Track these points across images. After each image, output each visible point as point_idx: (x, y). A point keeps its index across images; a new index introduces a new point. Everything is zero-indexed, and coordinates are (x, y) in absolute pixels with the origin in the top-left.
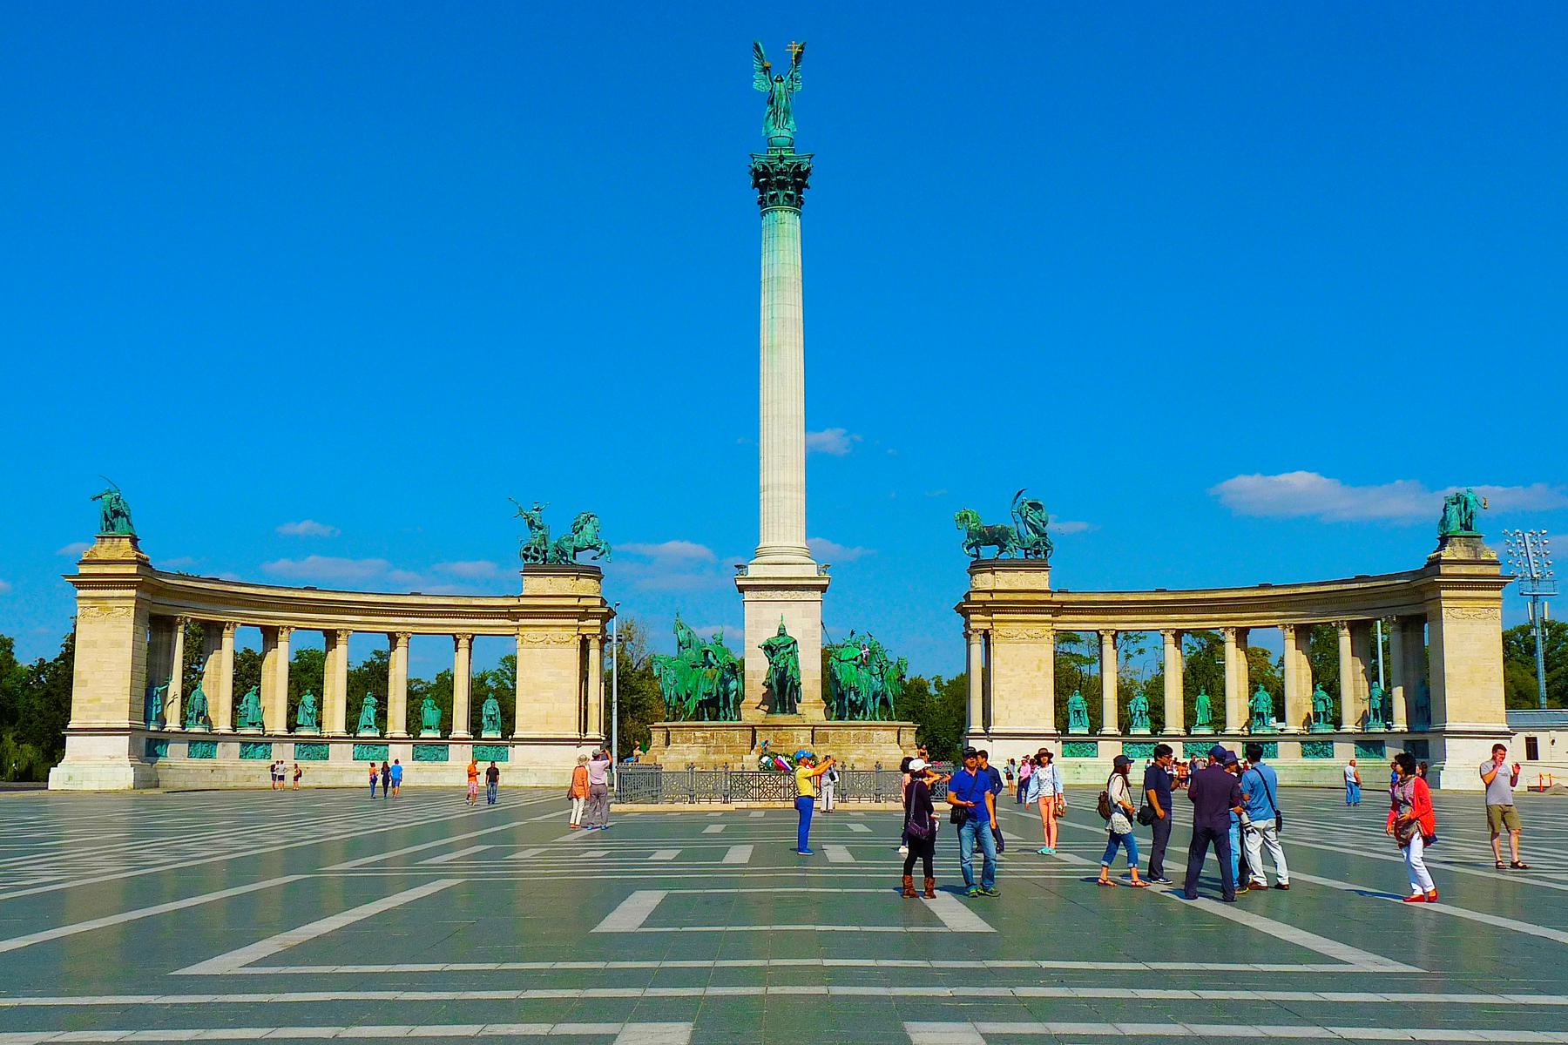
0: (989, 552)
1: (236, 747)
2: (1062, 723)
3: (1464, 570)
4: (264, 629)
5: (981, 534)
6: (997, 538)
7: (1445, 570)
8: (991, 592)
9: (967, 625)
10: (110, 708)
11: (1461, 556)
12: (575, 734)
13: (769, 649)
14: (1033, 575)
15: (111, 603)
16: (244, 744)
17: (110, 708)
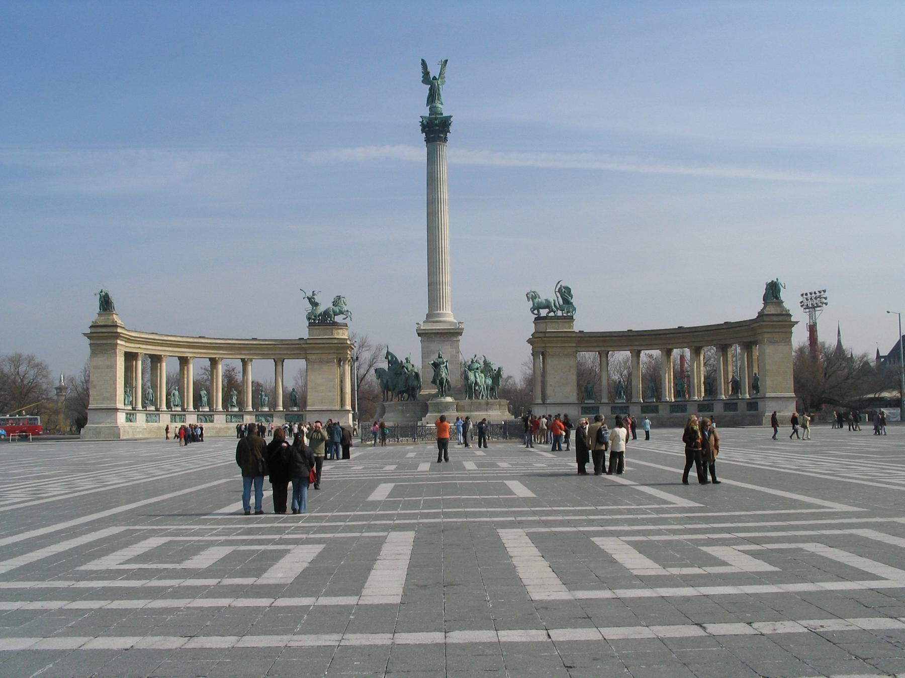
0: (544, 312)
2: (581, 400)
4: (180, 358)
6: (547, 306)
7: (766, 319)
10: (108, 399)
11: (773, 312)
12: (338, 407)
16: (172, 415)
17: (108, 399)
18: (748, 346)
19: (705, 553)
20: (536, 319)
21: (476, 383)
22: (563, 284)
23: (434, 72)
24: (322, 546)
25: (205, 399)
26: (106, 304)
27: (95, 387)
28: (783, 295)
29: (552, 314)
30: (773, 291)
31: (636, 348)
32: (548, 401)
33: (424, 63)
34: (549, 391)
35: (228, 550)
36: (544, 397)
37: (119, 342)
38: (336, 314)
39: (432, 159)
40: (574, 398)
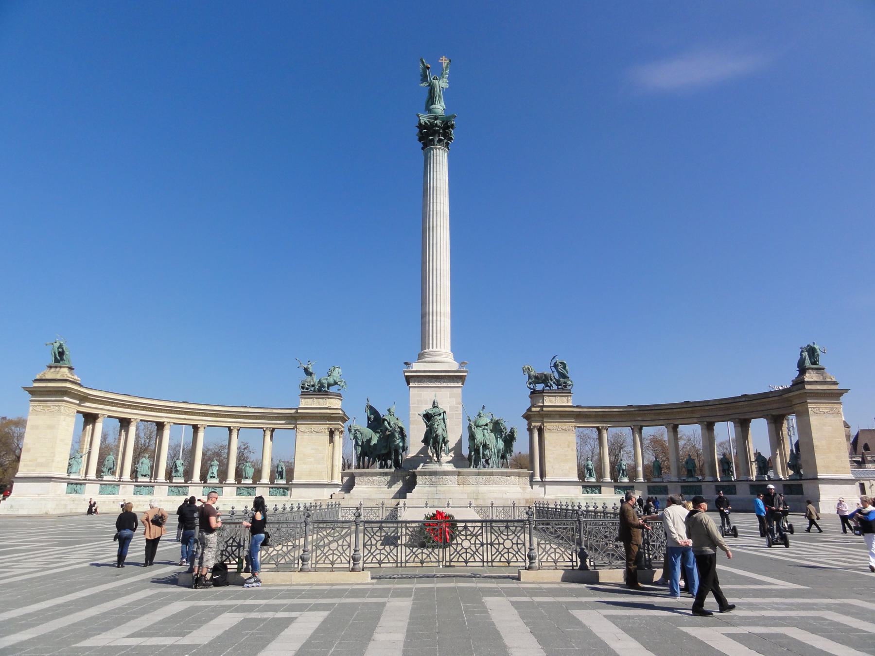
0: (539, 387)
1: (131, 488)
2: (581, 475)
3: (819, 387)
5: (536, 377)
7: (808, 387)
8: (542, 407)
9: (529, 424)
13: (428, 417)
14: (564, 399)
15: (49, 404)
18: (776, 422)
19: (686, 634)
20: (532, 393)
21: (485, 446)
22: (558, 360)
24: (326, 614)
25: (181, 469)
26: (60, 357)
27: (29, 450)
31: (638, 423)
32: (547, 479)
34: (548, 468)
35: (239, 617)
36: (543, 474)
37: (66, 398)
38: (329, 385)
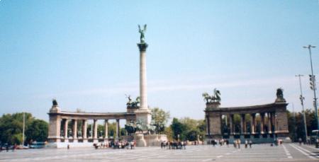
22: (217, 89)
23: (142, 28)
26: (55, 103)
28: (284, 93)
29: (213, 101)
30: (280, 92)
33: (139, 27)
39: (141, 56)
40: (220, 132)
